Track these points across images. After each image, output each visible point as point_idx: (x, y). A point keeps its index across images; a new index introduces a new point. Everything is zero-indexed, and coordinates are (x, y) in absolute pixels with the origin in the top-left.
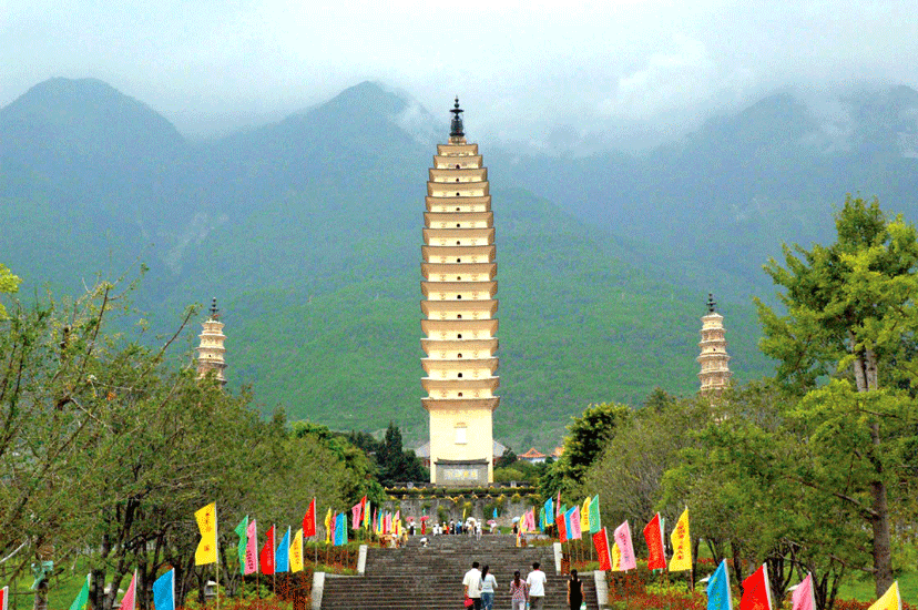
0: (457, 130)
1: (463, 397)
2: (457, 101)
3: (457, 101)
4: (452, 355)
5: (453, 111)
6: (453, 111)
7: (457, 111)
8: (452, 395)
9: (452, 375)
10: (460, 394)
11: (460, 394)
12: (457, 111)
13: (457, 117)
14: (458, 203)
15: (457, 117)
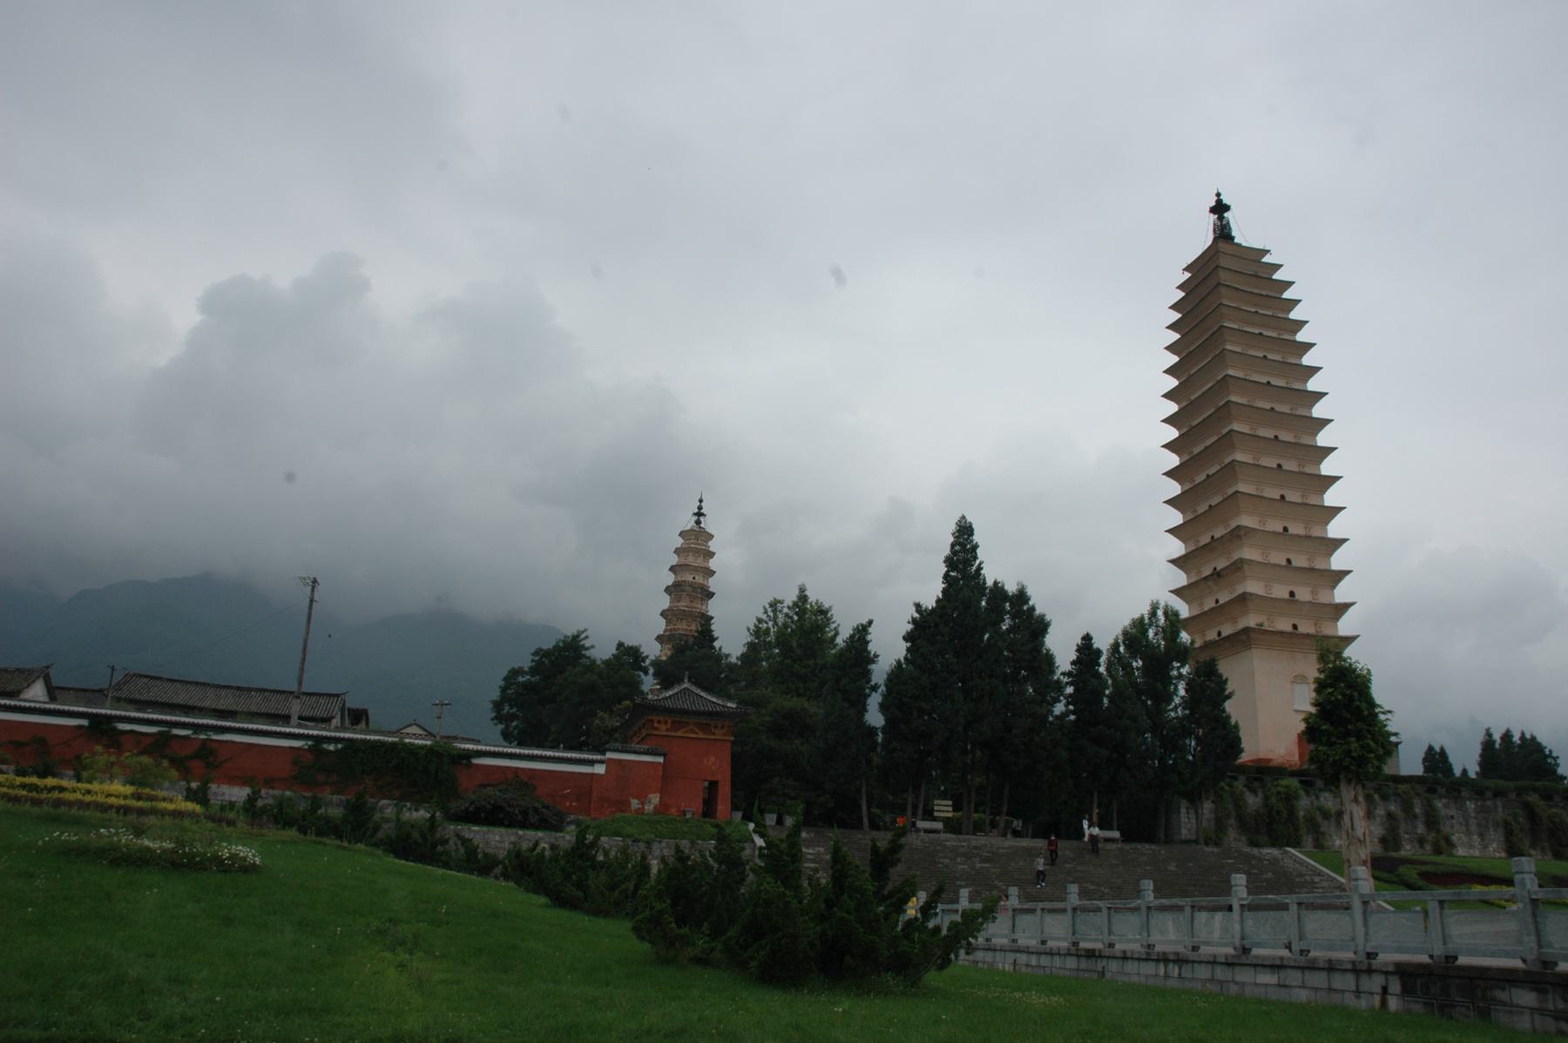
0: (1223, 233)
1: (1301, 629)
2: (1218, 195)
3: (1218, 195)
4: (1278, 558)
5: (1213, 210)
6: (1213, 210)
7: (1220, 208)
8: (1284, 625)
9: (1281, 592)
10: (1295, 627)
11: (1295, 627)
12: (1220, 208)
13: (1221, 218)
14: (1263, 326)
15: (1221, 218)
